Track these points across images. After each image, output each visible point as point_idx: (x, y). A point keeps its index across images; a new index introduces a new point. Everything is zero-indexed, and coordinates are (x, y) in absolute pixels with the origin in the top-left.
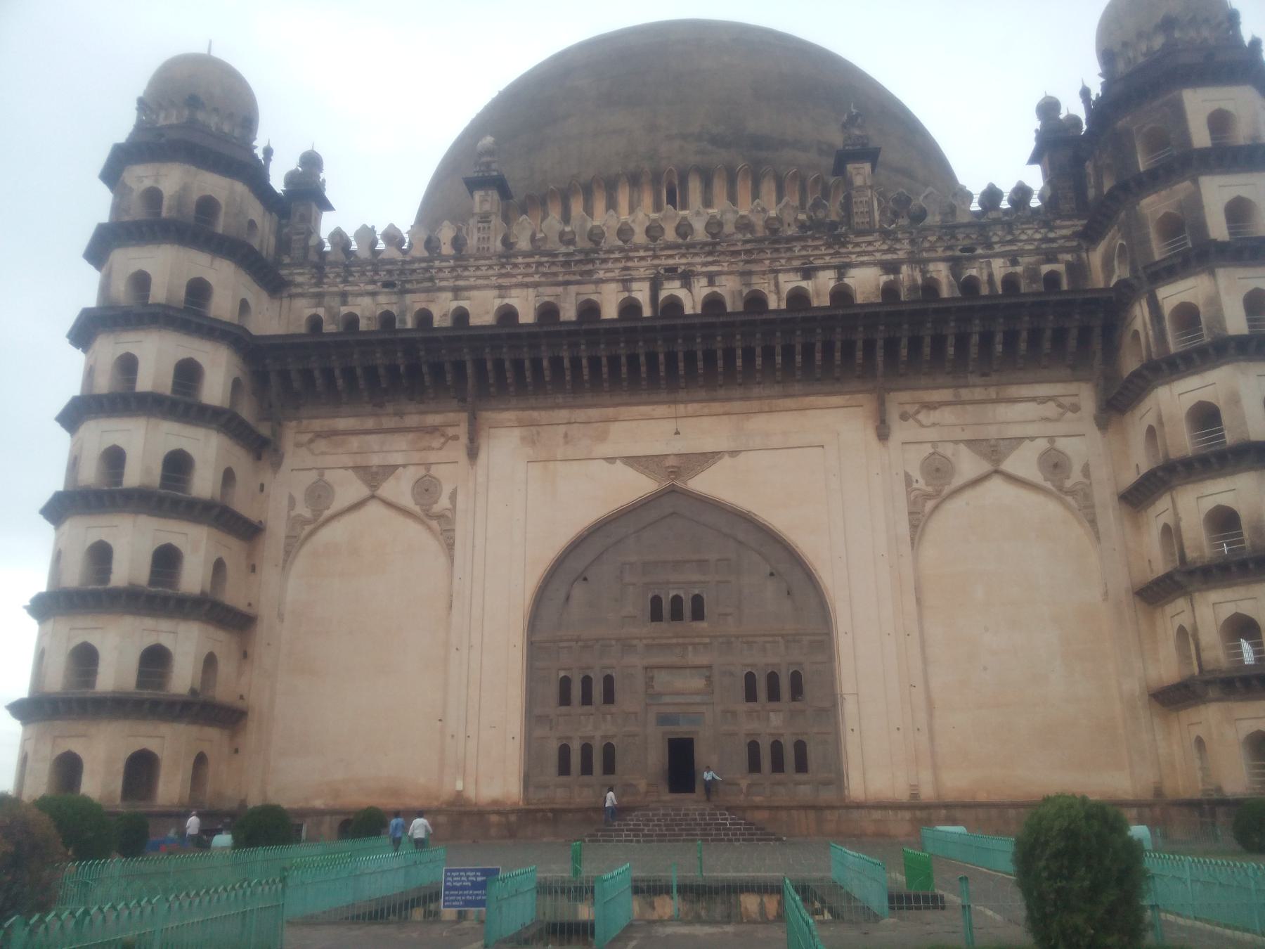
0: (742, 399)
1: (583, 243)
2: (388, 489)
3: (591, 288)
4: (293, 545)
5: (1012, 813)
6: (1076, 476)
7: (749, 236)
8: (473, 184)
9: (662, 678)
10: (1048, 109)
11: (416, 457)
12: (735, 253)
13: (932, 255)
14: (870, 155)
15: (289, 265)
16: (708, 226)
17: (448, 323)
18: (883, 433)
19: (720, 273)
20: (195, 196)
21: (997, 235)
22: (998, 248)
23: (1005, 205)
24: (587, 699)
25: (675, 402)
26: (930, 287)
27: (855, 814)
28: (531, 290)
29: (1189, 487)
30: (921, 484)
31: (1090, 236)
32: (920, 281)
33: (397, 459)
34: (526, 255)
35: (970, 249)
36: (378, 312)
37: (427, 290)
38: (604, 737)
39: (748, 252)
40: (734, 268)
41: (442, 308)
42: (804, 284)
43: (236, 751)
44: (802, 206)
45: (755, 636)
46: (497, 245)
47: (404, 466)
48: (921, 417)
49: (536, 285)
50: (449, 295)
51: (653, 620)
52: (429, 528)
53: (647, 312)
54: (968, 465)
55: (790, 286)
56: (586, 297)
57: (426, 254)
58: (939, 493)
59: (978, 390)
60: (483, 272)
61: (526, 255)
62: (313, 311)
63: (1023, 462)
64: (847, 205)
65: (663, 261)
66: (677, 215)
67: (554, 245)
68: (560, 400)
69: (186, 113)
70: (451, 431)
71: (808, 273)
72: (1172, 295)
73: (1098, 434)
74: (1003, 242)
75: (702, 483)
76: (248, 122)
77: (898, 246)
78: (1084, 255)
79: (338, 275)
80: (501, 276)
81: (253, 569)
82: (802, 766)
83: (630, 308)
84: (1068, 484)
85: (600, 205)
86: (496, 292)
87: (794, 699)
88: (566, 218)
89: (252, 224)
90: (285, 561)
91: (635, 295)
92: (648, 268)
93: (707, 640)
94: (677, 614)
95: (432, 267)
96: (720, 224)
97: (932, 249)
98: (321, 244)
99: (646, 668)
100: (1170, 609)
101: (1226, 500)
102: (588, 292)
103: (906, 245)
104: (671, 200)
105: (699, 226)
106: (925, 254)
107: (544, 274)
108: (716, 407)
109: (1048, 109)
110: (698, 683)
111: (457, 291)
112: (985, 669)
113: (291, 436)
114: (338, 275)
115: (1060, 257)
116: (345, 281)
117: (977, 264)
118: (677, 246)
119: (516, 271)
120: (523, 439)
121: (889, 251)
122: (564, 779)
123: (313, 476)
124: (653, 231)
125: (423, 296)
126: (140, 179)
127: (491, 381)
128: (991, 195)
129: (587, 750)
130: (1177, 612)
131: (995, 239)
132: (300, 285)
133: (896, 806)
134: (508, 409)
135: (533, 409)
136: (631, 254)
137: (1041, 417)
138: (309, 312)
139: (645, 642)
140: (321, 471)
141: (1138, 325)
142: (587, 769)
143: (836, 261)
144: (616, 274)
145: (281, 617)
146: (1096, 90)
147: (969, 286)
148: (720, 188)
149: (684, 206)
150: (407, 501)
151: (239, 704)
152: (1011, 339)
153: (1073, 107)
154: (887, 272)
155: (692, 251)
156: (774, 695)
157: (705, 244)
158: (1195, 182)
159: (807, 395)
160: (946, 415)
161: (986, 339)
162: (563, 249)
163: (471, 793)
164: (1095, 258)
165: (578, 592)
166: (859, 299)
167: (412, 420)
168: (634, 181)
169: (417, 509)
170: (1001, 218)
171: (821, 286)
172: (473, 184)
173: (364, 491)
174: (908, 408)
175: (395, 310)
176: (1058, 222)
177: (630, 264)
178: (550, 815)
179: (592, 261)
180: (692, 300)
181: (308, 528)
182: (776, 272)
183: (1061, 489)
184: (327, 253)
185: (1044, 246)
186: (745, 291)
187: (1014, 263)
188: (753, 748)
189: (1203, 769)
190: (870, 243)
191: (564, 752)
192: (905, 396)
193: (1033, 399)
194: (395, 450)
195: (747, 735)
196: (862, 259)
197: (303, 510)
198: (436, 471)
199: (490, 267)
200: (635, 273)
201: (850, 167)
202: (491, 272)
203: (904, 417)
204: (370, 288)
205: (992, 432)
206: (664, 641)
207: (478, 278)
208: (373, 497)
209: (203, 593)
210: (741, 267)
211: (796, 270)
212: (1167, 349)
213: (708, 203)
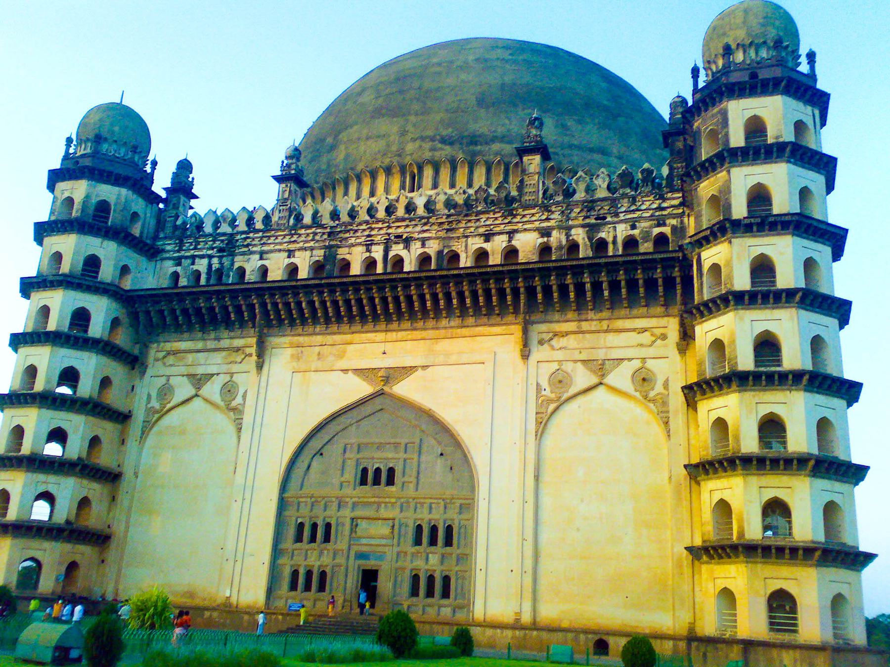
0: (433, 328)
2: (206, 390)
3: (346, 250)
4: (148, 427)
5: (582, 637)
6: (659, 388)
13: (576, 222)
19: (429, 238)
20: (94, 201)
21: (624, 205)
24: (313, 539)
26: (573, 247)
28: (308, 253)
29: (705, 401)
30: (547, 393)
32: (564, 242)
34: (308, 227)
35: (605, 218)
37: (243, 254)
38: (320, 567)
39: (451, 222)
40: (442, 234)
41: (251, 265)
43: (103, 561)
45: (425, 498)
47: (218, 374)
48: (553, 342)
49: (312, 249)
50: (257, 256)
52: (229, 418)
53: (380, 269)
54: (582, 378)
56: (342, 257)
57: (246, 229)
59: (595, 323)
62: (174, 269)
64: (521, 188)
66: (407, 198)
67: (326, 220)
68: (318, 329)
70: (248, 350)
71: (488, 237)
75: (402, 389)
77: (552, 217)
78: (686, 220)
81: (123, 443)
82: (446, 594)
83: (371, 264)
84: (652, 394)
90: (141, 437)
91: (373, 255)
93: (393, 500)
94: (377, 481)
95: (248, 238)
96: (435, 203)
97: (576, 218)
99: (353, 519)
106: (570, 223)
107: (318, 241)
108: (418, 334)
110: (386, 531)
111: (262, 255)
112: (578, 529)
113: (153, 352)
114: (191, 245)
115: (668, 222)
116: (195, 248)
117: (606, 229)
118: (403, 220)
120: (292, 356)
121: (548, 219)
122: (293, 593)
123: (163, 380)
124: (390, 210)
127: (272, 317)
129: (309, 574)
131: (623, 209)
132: (169, 251)
133: (502, 626)
134: (284, 336)
135: (299, 335)
136: (373, 226)
137: (642, 341)
139: (354, 500)
142: (308, 588)
143: (509, 228)
144: (363, 239)
145: (136, 474)
147: (601, 245)
148: (445, 174)
152: (615, 286)
154: (542, 237)
155: (413, 223)
156: (433, 542)
157: (422, 218)
158: (729, 172)
159: (477, 326)
160: (571, 341)
161: (597, 287)
163: (234, 600)
166: (522, 258)
167: (225, 343)
168: (388, 171)
169: (222, 404)
171: (496, 247)
173: (193, 392)
176: (669, 195)
177: (373, 233)
178: (280, 617)
179: (348, 231)
182: (467, 237)
185: (657, 214)
186: (446, 251)
187: (633, 227)
188: (416, 578)
190: (533, 215)
191: (295, 574)
192: (543, 327)
193: (634, 330)
194: (213, 363)
195: (412, 570)
196: (526, 227)
198: (236, 378)
199: (285, 236)
200: (376, 239)
202: (285, 240)
203: (541, 343)
204: (210, 252)
205: (600, 355)
206: (365, 500)
208: (197, 395)
209: (79, 458)
211: (481, 235)
212: (703, 298)
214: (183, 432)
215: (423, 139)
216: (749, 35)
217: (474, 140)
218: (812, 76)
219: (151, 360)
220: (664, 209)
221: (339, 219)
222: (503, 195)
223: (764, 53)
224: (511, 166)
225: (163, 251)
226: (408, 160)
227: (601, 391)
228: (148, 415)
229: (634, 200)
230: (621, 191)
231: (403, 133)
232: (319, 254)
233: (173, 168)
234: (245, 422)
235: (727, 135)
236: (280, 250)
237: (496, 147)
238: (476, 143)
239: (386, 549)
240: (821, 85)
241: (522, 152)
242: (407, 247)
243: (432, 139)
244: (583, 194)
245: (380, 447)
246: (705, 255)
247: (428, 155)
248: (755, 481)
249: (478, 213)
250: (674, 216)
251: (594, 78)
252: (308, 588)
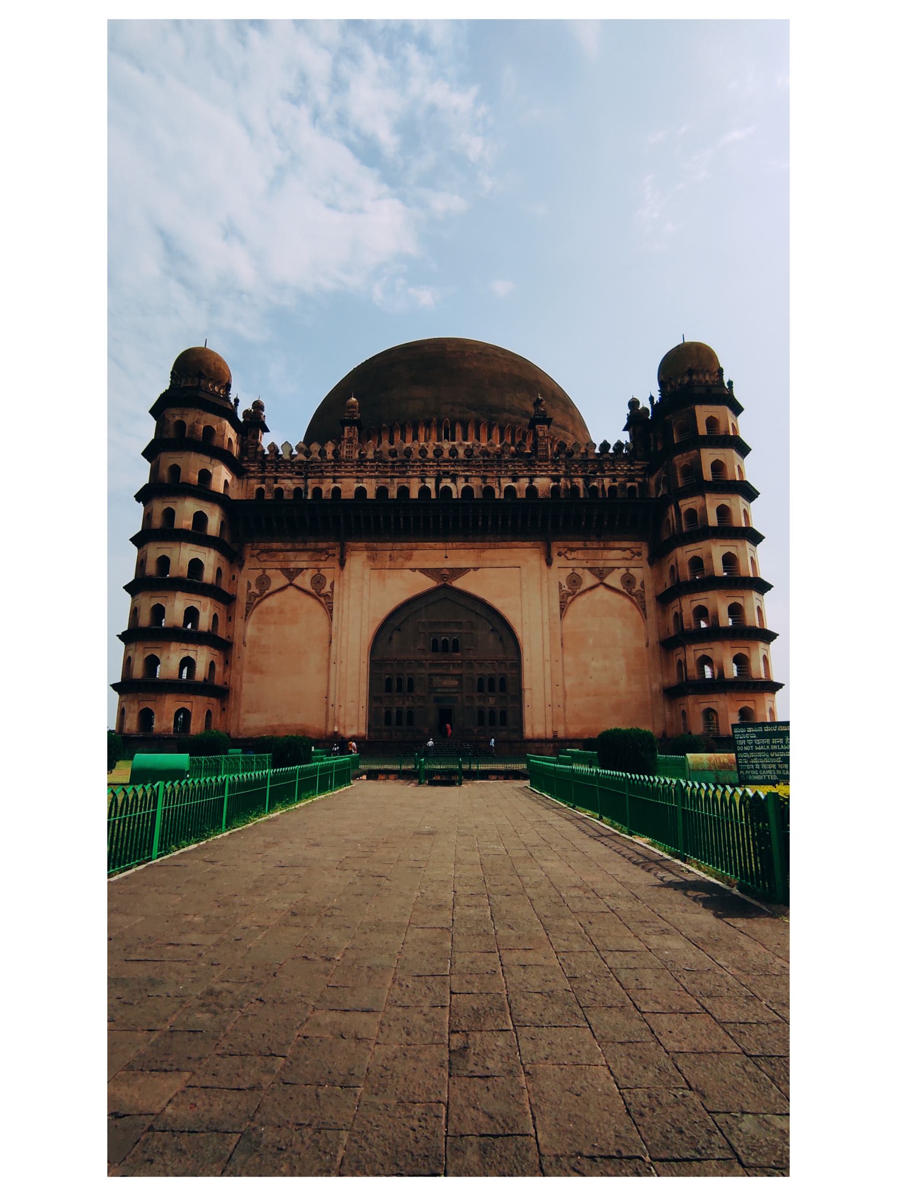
1: (400, 457)
2: (298, 581)
3: (405, 480)
6: (638, 587)
7: (486, 458)
9: (436, 680)
10: (633, 404)
11: (313, 564)
12: (479, 466)
14: (548, 422)
15: (247, 461)
16: (466, 451)
17: (330, 496)
18: (549, 563)
19: (471, 476)
22: (607, 473)
23: (611, 451)
24: (400, 689)
25: (447, 541)
26: (575, 489)
27: (529, 745)
30: (566, 588)
33: (303, 565)
36: (293, 487)
37: (320, 477)
41: (327, 486)
42: (513, 484)
43: (224, 709)
44: (513, 443)
46: (357, 456)
48: (567, 555)
49: (376, 477)
50: (331, 480)
51: (433, 651)
52: (320, 601)
53: (433, 496)
54: (589, 580)
58: (574, 593)
60: (349, 469)
61: (371, 461)
63: (614, 580)
65: (443, 469)
69: (197, 380)
70: (331, 552)
72: (686, 504)
73: (649, 567)
74: (609, 470)
75: (458, 584)
76: (228, 387)
79: (273, 468)
80: (358, 471)
81: (230, 620)
83: (424, 491)
84: (634, 591)
85: (409, 437)
86: (355, 480)
87: (501, 691)
89: (230, 439)
92: (434, 471)
96: (472, 451)
98: (264, 451)
99: (430, 675)
100: (675, 652)
101: (703, 603)
102: (404, 482)
104: (446, 437)
105: (461, 452)
108: (468, 545)
109: (633, 404)
111: (335, 479)
113: (248, 552)
114: (273, 468)
115: (636, 479)
116: (276, 471)
119: (365, 470)
120: (368, 557)
121: (556, 470)
123: (260, 572)
124: (438, 452)
125: (317, 480)
128: (605, 446)
129: (399, 713)
130: (678, 654)
132: (253, 472)
138: (257, 487)
140: (264, 570)
141: (670, 517)
145: (244, 643)
146: (657, 399)
149: (453, 440)
150: (308, 586)
151: (225, 686)
153: (645, 404)
158: (699, 451)
160: (579, 555)
162: (391, 459)
165: (396, 636)
166: (540, 494)
169: (314, 591)
170: (608, 456)
172: (344, 423)
173: (287, 582)
174: (561, 550)
175: (302, 487)
179: (406, 466)
180: (456, 489)
181: (258, 599)
183: (630, 593)
184: (267, 455)
186: (484, 486)
189: (684, 724)
190: (546, 466)
192: (560, 544)
194: (301, 561)
197: (254, 590)
199: (352, 467)
201: (537, 426)
203: (560, 554)
204: (289, 475)
205: (601, 564)
207: (346, 472)
208: (291, 584)
211: (510, 477)
214: (281, 612)
219: (248, 556)
220: (633, 471)
221: (396, 456)
223: (707, 378)
225: (248, 471)
227: (601, 589)
228: (250, 599)
229: (613, 463)
230: (605, 456)
232: (382, 482)
233: (249, 407)
234: (335, 606)
236: (350, 477)
239: (457, 695)
242: (454, 481)
244: (579, 456)
245: (446, 624)
246: (681, 503)
248: (728, 644)
249: (506, 461)
250: (640, 476)
252: (399, 722)
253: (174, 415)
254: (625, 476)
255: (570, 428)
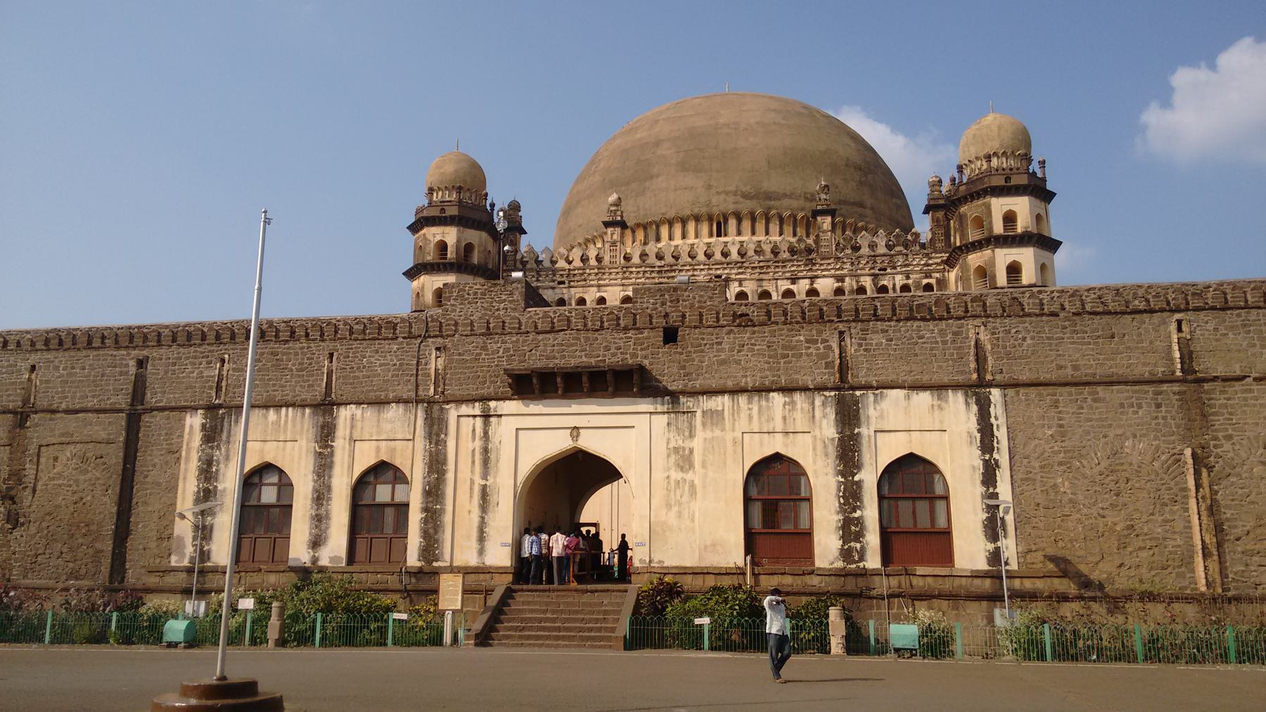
1: (669, 259)
8: (607, 224)
12: (753, 268)
26: (862, 290)
31: (950, 263)
39: (761, 267)
41: (591, 295)
50: (595, 289)
55: (784, 288)
65: (713, 272)
67: (652, 260)
71: (794, 280)
85: (678, 230)
88: (658, 239)
103: (848, 266)
111: (599, 286)
116: (538, 280)
126: (434, 235)
147: (884, 289)
148: (746, 224)
162: (658, 263)
164: (952, 275)
168: (697, 219)
172: (607, 224)
201: (819, 218)
210: (756, 276)
213: (739, 233)
215: (727, 193)
216: (1002, 146)
217: (769, 196)
218: (1044, 180)
222: (803, 246)
224: (809, 223)
226: (716, 211)
231: (709, 187)
235: (991, 223)
236: (616, 285)
237: (786, 202)
238: (770, 198)
240: (1049, 187)
241: (816, 213)
243: (735, 194)
247: (731, 208)
251: (847, 140)
253: (434, 234)
254: (921, 271)
255: (868, 203)
